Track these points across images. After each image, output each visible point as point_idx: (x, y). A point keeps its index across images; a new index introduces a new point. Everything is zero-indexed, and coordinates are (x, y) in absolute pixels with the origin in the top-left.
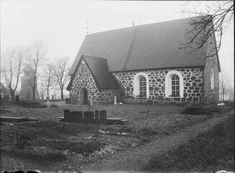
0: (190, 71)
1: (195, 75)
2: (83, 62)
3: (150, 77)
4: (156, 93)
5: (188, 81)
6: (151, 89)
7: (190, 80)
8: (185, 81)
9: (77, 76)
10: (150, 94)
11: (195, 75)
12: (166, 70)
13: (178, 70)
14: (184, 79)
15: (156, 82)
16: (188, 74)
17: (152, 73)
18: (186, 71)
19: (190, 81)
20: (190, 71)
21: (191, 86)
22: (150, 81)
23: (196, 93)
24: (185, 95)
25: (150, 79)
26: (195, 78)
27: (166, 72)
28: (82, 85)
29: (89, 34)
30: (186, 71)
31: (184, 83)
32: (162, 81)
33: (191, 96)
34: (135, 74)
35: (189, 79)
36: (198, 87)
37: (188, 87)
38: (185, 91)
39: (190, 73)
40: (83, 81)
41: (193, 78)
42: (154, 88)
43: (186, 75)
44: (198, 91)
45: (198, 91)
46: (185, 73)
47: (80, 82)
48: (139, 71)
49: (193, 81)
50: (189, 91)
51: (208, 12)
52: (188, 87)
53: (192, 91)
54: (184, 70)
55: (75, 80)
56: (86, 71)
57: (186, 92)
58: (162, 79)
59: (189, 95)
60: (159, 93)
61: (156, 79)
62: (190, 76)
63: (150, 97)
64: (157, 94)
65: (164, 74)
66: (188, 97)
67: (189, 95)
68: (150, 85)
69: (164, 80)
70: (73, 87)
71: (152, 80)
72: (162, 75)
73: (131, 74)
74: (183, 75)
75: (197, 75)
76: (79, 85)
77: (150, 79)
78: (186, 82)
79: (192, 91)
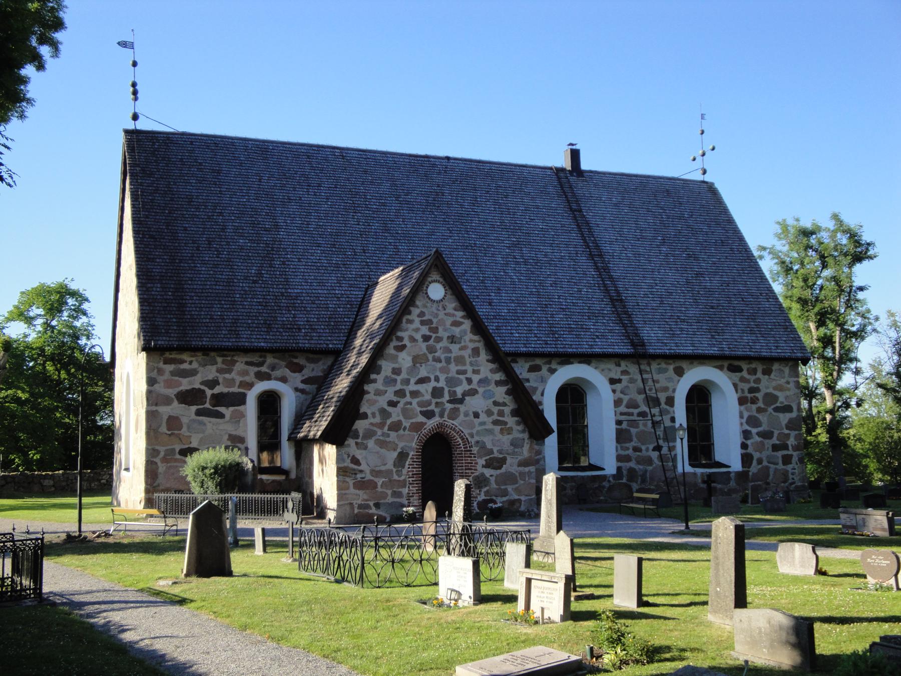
0: (759, 375)
1: (775, 388)
2: (436, 291)
3: (618, 387)
4: (644, 453)
5: (754, 407)
6: (622, 436)
7: (761, 404)
8: (743, 408)
9: (394, 359)
10: (619, 458)
11: (775, 388)
12: (679, 363)
13: (721, 368)
14: (742, 401)
15: (644, 408)
16: (756, 386)
17: (625, 372)
18: (745, 374)
19: (759, 410)
20: (759, 375)
21: (764, 427)
22: (617, 403)
23: (780, 454)
24: (746, 459)
25: (619, 395)
26: (776, 398)
27: (680, 372)
28: (429, 415)
29: (143, 125)
30: (745, 374)
31: (741, 417)
32: (663, 406)
33: (765, 463)
34: (552, 371)
35: (754, 401)
36: (787, 432)
37: (754, 431)
38: (744, 446)
39: (758, 381)
40: (437, 393)
41: (770, 399)
42: (633, 431)
43: (746, 386)
44: (785, 447)
45: (785, 447)
46: (743, 380)
47: (415, 394)
48: (567, 358)
49: (770, 410)
50: (760, 447)
51: (704, 172)
52: (754, 431)
53: (769, 443)
54: (739, 370)
55: (379, 385)
56: (452, 339)
57: (750, 450)
58: (662, 397)
59: (760, 461)
60: (655, 455)
61: (640, 398)
62: (757, 390)
63: (619, 469)
64: (649, 461)
65: (670, 379)
66: (754, 468)
67: (760, 461)
68: (619, 423)
69: (670, 401)
70: (361, 425)
71: (626, 399)
72: (663, 383)
73: (534, 369)
74: (735, 386)
75: (780, 388)
76: (406, 413)
77: (619, 395)
78: (746, 415)
79: (769, 443)
